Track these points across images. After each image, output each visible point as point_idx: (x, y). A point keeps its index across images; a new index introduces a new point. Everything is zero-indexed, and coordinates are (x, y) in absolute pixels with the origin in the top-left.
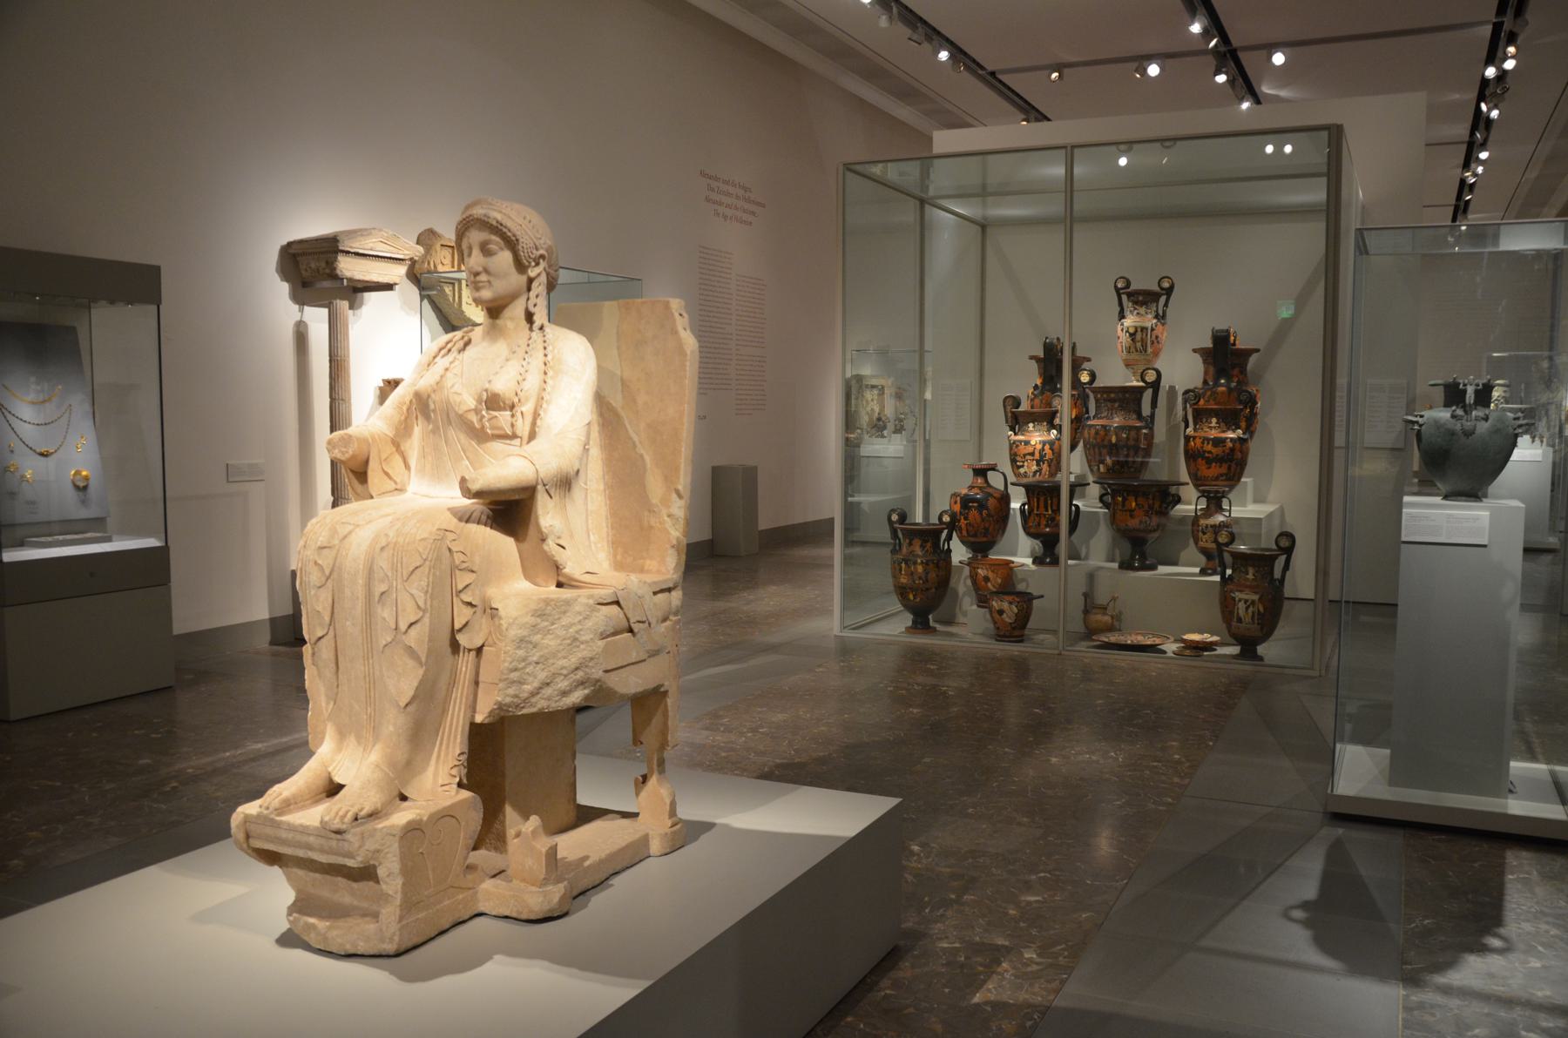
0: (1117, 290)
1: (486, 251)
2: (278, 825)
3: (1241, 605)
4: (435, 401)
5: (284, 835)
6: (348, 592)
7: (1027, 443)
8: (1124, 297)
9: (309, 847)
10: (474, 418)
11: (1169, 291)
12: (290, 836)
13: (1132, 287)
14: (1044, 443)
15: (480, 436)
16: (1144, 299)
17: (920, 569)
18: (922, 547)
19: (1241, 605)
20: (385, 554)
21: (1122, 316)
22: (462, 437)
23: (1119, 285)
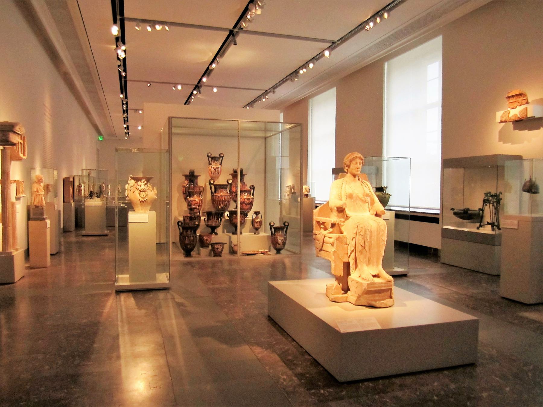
0: (208, 156)
1: (360, 164)
3: (280, 241)
4: (354, 195)
5: (376, 285)
7: (195, 200)
8: (210, 159)
9: (382, 286)
10: (363, 199)
11: (223, 157)
13: (212, 156)
14: (200, 200)
15: (365, 202)
16: (214, 159)
17: (192, 238)
18: (191, 231)
19: (280, 241)
21: (210, 164)
23: (209, 155)
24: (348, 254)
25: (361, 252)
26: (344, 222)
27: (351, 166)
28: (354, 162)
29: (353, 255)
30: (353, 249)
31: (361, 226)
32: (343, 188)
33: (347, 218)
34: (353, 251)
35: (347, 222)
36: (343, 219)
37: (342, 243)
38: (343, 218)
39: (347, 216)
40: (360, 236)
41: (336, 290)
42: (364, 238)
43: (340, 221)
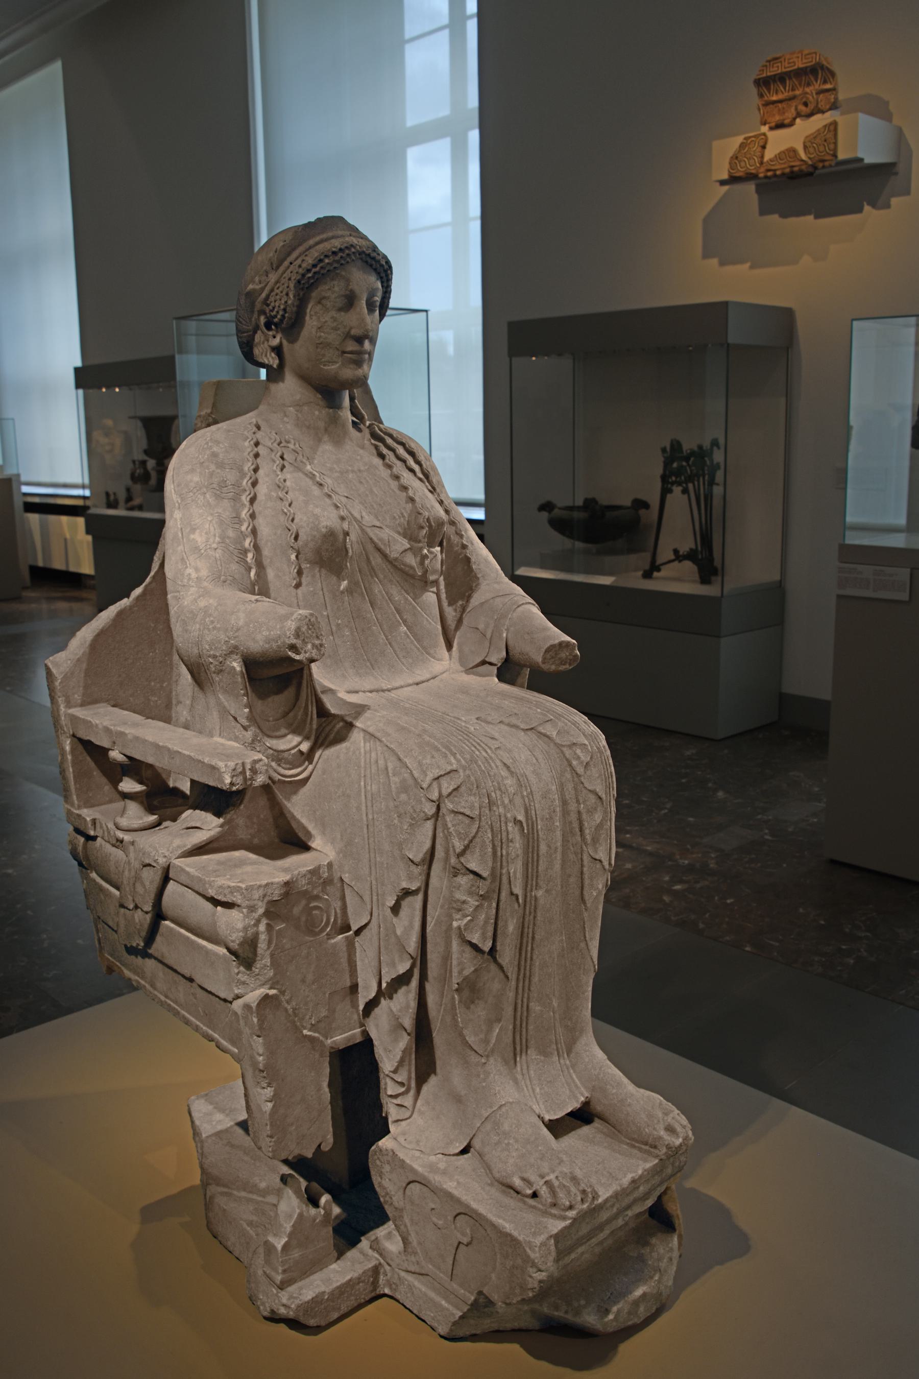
2: (601, 1207)
5: (605, 1216)
6: (543, 848)
10: (411, 560)
12: (615, 1210)
15: (418, 582)
20: (594, 772)
22: (397, 594)
24: (354, 989)
25: (470, 990)
26: (308, 757)
27: (311, 323)
28: (332, 290)
29: (403, 1003)
30: (403, 968)
31: (469, 803)
32: (262, 490)
33: (328, 728)
34: (402, 980)
35: (326, 756)
36: (291, 742)
37: (311, 928)
38: (296, 731)
39: (323, 712)
40: (464, 880)
41: (296, 1254)
42: (492, 889)
43: (278, 756)
